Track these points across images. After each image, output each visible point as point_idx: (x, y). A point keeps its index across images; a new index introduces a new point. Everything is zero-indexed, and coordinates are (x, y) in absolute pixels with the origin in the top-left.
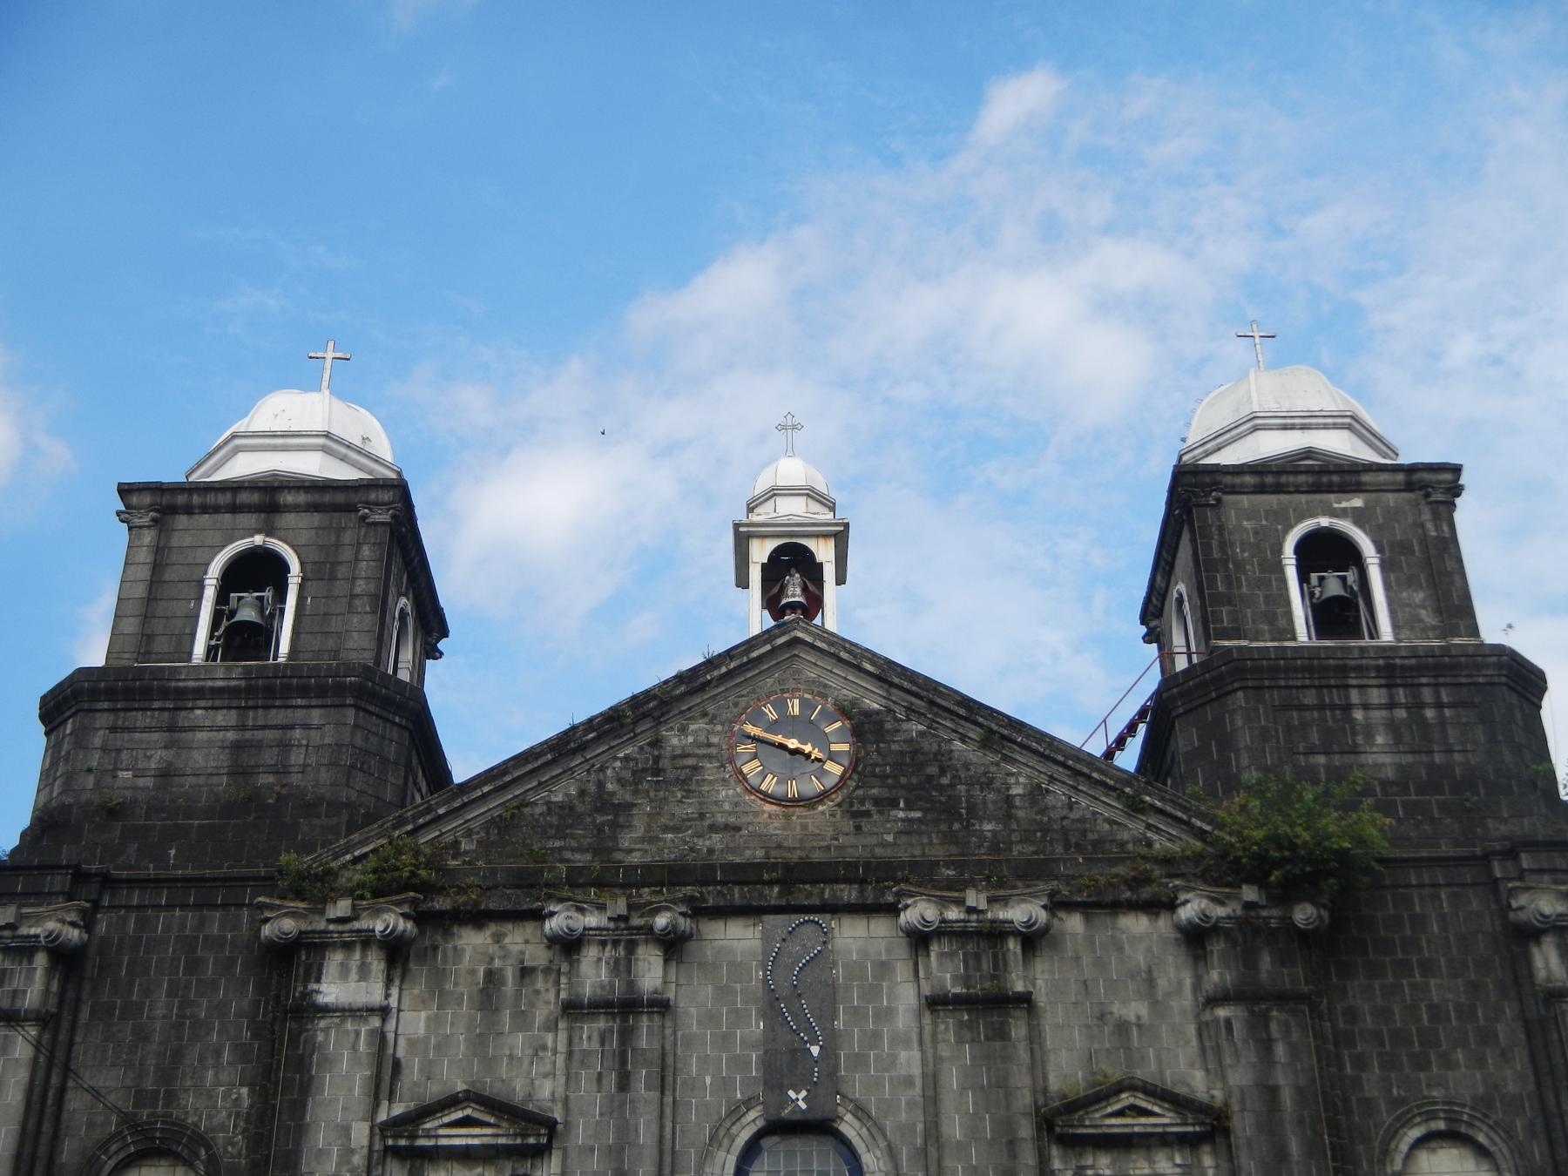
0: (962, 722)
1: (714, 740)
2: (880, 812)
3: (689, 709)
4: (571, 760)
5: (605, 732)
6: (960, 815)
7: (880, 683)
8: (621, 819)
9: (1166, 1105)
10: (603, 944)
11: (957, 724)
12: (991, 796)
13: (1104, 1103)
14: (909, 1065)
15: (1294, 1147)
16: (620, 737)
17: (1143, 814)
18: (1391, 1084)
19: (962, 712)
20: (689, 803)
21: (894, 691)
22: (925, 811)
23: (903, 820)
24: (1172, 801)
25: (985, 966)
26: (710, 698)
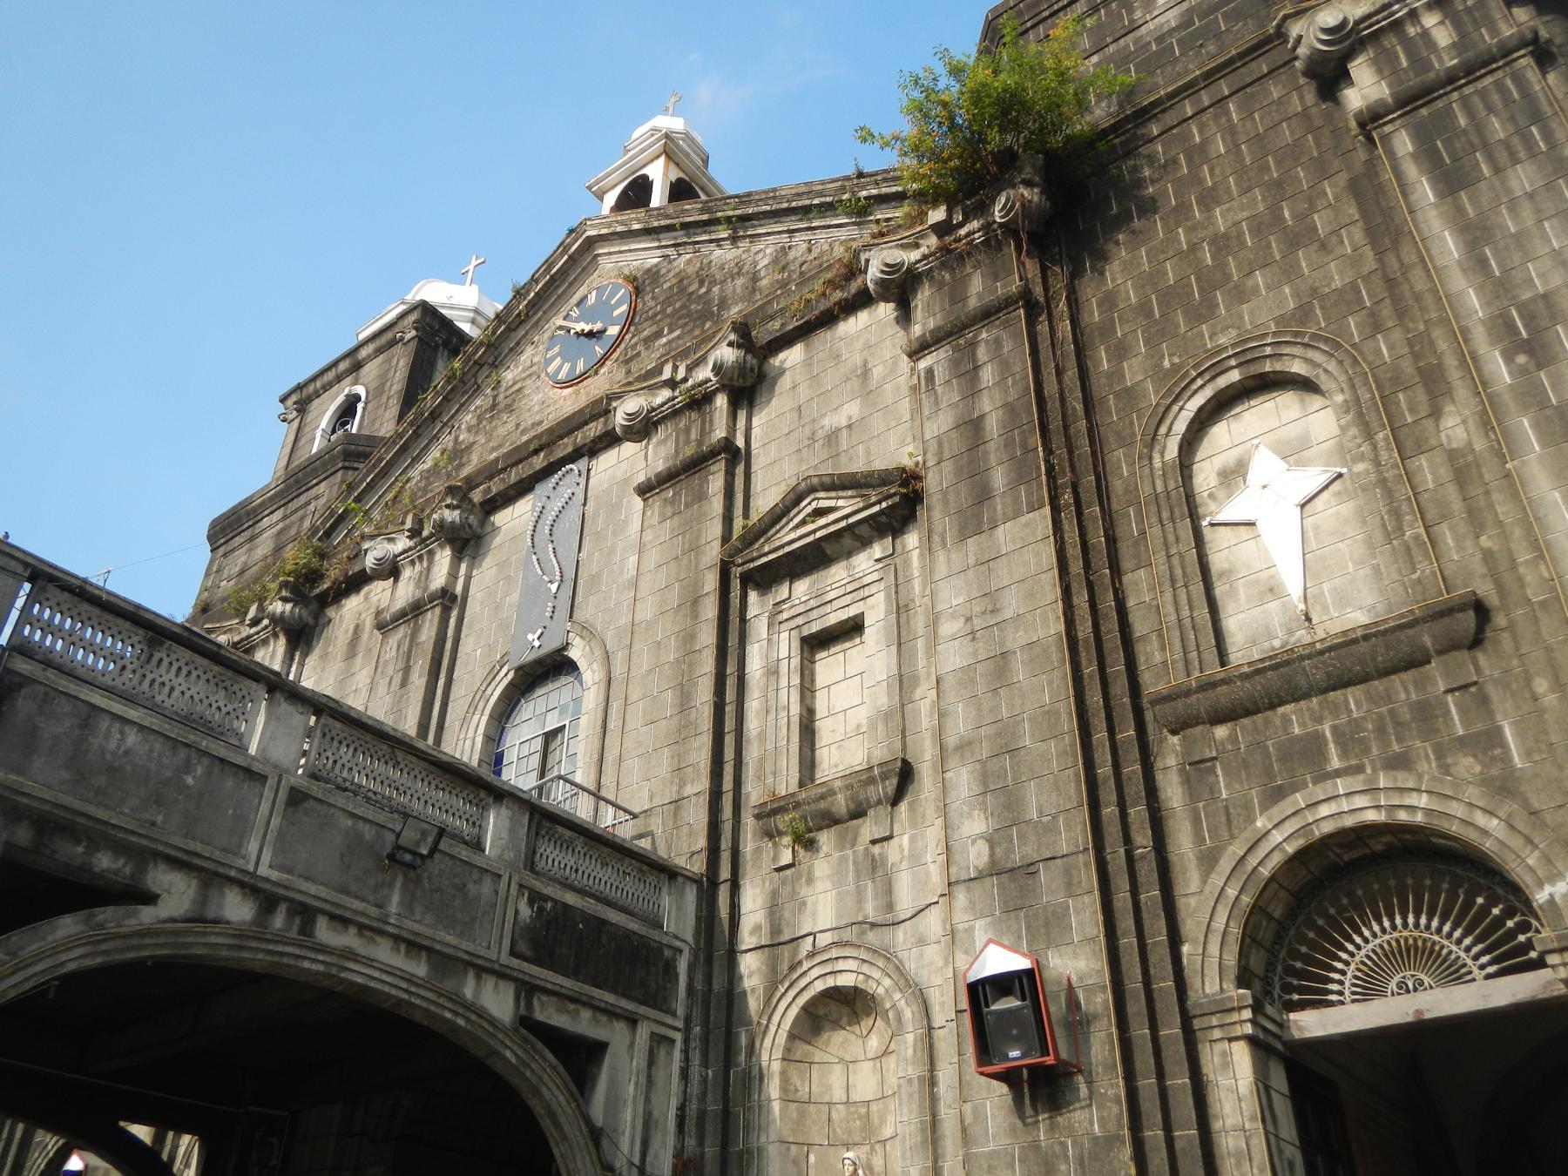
0: (713, 228)
4: (433, 429)
5: (449, 393)
6: (712, 312)
8: (464, 460)
9: (850, 493)
10: (413, 563)
11: (710, 233)
12: (740, 282)
13: (784, 520)
15: (999, 478)
17: (871, 214)
18: (1163, 356)
19: (705, 217)
21: (661, 236)
23: (665, 345)
24: (885, 180)
25: (693, 437)
26: (532, 327)
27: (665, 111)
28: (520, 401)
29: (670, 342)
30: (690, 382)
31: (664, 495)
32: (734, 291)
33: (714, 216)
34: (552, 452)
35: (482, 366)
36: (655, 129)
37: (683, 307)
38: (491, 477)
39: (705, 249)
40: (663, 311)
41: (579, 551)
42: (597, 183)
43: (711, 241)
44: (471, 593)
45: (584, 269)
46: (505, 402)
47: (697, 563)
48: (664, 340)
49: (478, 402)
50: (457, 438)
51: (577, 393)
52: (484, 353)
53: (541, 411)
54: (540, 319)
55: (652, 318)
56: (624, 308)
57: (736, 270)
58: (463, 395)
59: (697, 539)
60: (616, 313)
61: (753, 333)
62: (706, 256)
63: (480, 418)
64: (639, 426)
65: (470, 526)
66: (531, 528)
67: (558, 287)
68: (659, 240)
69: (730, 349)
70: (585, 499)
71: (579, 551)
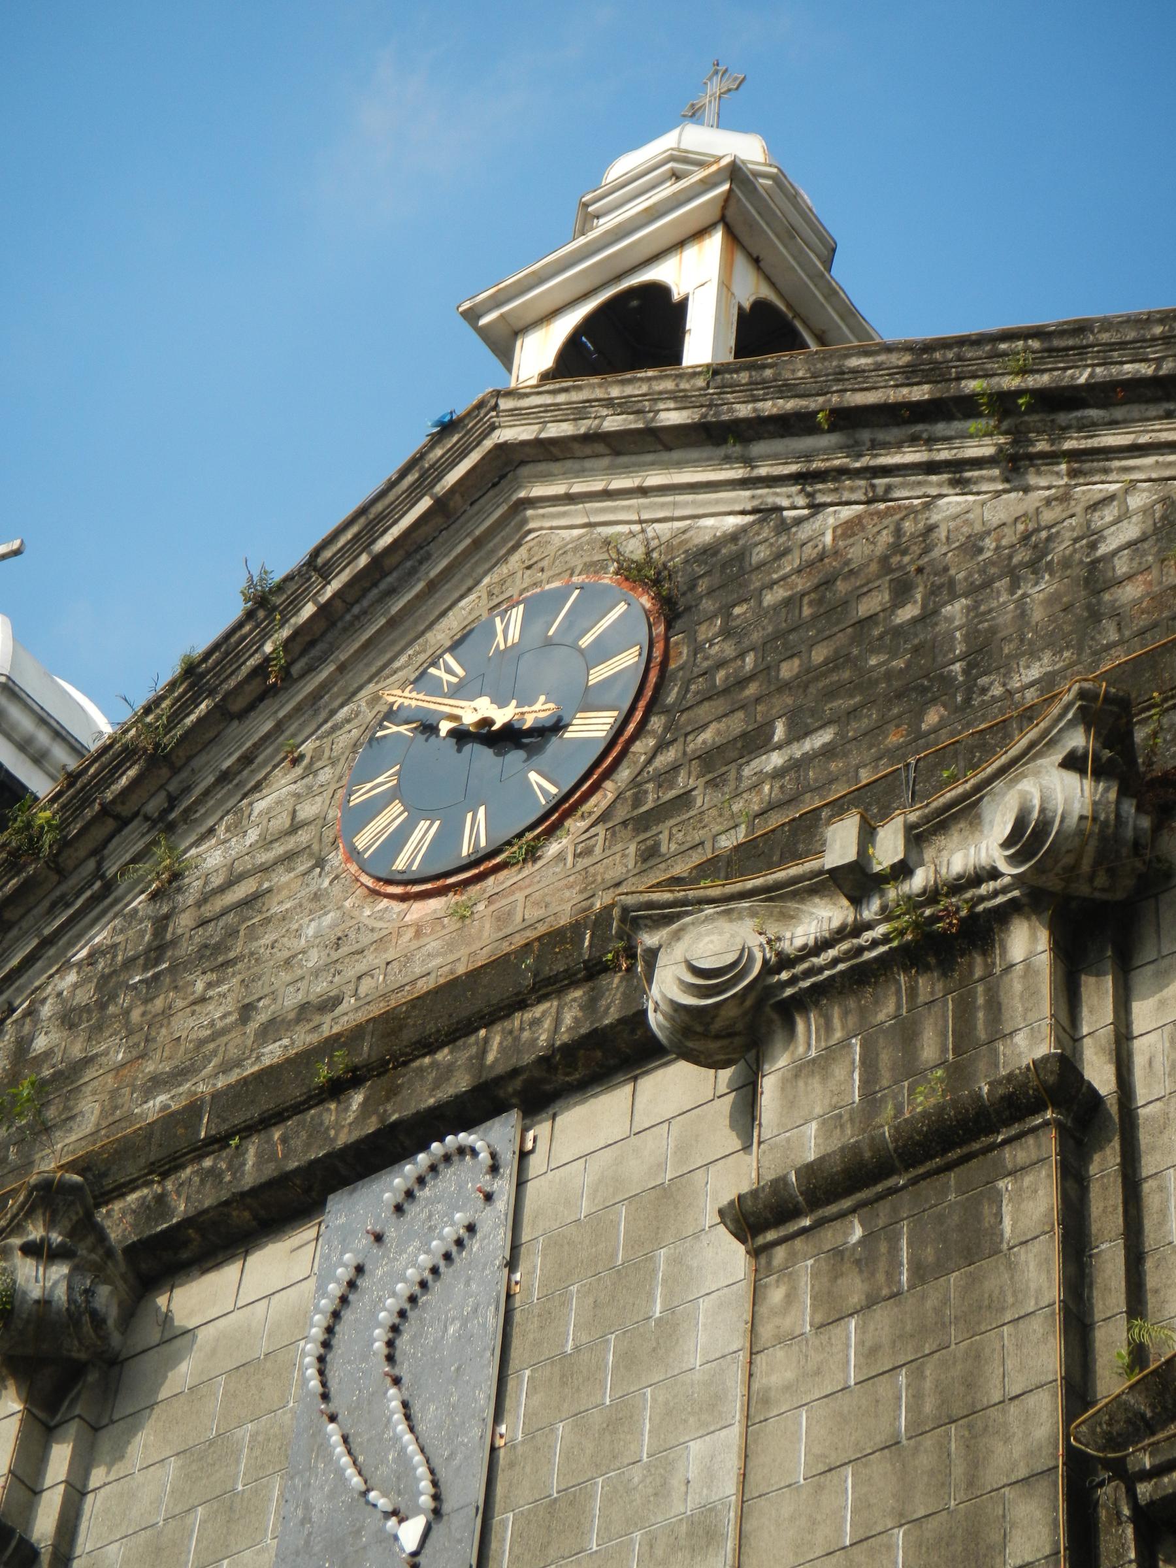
0: (940, 428)
1: (307, 811)
2: (713, 784)
3: (247, 760)
6: (947, 681)
7: (722, 451)
8: (51, 1113)
11: (930, 441)
14: (710, 1477)
16: (68, 905)
19: (920, 393)
20: (219, 995)
21: (757, 448)
22: (840, 720)
23: (778, 774)
25: (929, 1050)
26: (298, 709)
27: (694, 115)
28: (252, 934)
29: (795, 766)
30: (919, 880)
31: (829, 1237)
32: (1022, 614)
33: (952, 389)
34: (393, 1092)
35: (124, 822)
36: (681, 161)
37: (834, 662)
38: (168, 1167)
39: (907, 493)
40: (765, 671)
41: (498, 1418)
42: (496, 301)
43: (931, 468)
44: (85, 1542)
45: (478, 544)
46: (199, 936)
47: (975, 1464)
48: (776, 759)
49: (101, 937)
50: (22, 1046)
51: (463, 916)
52: (135, 783)
53: (332, 967)
54: (324, 688)
55: (726, 691)
56: (628, 659)
57: (1022, 556)
58: (52, 911)
59: (970, 1383)
60: (598, 675)
61: (1140, 735)
62: (912, 511)
63: (108, 988)
64: (732, 1012)
65: (98, 1320)
66: (317, 1332)
67: (392, 592)
68: (748, 462)
69: (1071, 779)
70: (515, 1247)
71: (498, 1418)
